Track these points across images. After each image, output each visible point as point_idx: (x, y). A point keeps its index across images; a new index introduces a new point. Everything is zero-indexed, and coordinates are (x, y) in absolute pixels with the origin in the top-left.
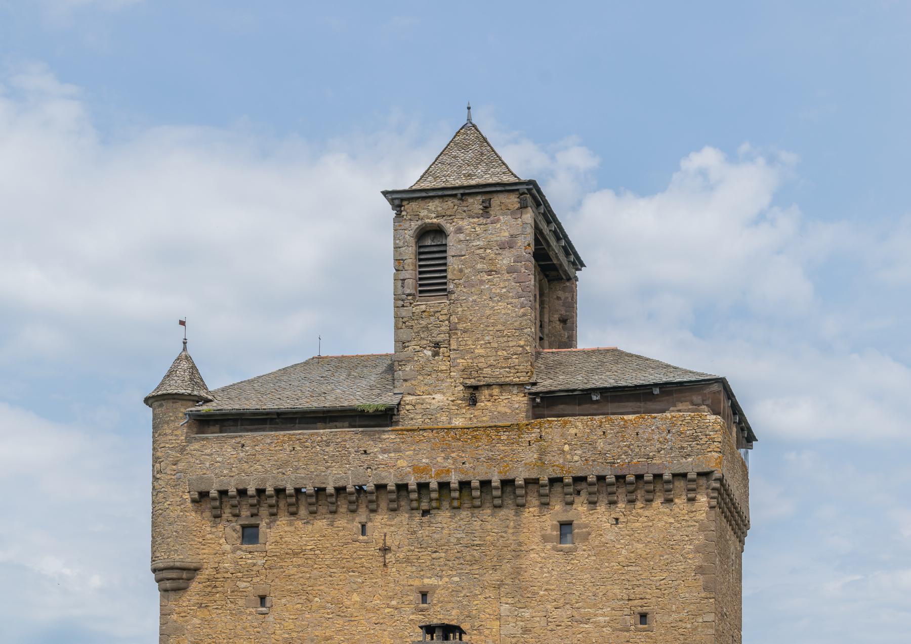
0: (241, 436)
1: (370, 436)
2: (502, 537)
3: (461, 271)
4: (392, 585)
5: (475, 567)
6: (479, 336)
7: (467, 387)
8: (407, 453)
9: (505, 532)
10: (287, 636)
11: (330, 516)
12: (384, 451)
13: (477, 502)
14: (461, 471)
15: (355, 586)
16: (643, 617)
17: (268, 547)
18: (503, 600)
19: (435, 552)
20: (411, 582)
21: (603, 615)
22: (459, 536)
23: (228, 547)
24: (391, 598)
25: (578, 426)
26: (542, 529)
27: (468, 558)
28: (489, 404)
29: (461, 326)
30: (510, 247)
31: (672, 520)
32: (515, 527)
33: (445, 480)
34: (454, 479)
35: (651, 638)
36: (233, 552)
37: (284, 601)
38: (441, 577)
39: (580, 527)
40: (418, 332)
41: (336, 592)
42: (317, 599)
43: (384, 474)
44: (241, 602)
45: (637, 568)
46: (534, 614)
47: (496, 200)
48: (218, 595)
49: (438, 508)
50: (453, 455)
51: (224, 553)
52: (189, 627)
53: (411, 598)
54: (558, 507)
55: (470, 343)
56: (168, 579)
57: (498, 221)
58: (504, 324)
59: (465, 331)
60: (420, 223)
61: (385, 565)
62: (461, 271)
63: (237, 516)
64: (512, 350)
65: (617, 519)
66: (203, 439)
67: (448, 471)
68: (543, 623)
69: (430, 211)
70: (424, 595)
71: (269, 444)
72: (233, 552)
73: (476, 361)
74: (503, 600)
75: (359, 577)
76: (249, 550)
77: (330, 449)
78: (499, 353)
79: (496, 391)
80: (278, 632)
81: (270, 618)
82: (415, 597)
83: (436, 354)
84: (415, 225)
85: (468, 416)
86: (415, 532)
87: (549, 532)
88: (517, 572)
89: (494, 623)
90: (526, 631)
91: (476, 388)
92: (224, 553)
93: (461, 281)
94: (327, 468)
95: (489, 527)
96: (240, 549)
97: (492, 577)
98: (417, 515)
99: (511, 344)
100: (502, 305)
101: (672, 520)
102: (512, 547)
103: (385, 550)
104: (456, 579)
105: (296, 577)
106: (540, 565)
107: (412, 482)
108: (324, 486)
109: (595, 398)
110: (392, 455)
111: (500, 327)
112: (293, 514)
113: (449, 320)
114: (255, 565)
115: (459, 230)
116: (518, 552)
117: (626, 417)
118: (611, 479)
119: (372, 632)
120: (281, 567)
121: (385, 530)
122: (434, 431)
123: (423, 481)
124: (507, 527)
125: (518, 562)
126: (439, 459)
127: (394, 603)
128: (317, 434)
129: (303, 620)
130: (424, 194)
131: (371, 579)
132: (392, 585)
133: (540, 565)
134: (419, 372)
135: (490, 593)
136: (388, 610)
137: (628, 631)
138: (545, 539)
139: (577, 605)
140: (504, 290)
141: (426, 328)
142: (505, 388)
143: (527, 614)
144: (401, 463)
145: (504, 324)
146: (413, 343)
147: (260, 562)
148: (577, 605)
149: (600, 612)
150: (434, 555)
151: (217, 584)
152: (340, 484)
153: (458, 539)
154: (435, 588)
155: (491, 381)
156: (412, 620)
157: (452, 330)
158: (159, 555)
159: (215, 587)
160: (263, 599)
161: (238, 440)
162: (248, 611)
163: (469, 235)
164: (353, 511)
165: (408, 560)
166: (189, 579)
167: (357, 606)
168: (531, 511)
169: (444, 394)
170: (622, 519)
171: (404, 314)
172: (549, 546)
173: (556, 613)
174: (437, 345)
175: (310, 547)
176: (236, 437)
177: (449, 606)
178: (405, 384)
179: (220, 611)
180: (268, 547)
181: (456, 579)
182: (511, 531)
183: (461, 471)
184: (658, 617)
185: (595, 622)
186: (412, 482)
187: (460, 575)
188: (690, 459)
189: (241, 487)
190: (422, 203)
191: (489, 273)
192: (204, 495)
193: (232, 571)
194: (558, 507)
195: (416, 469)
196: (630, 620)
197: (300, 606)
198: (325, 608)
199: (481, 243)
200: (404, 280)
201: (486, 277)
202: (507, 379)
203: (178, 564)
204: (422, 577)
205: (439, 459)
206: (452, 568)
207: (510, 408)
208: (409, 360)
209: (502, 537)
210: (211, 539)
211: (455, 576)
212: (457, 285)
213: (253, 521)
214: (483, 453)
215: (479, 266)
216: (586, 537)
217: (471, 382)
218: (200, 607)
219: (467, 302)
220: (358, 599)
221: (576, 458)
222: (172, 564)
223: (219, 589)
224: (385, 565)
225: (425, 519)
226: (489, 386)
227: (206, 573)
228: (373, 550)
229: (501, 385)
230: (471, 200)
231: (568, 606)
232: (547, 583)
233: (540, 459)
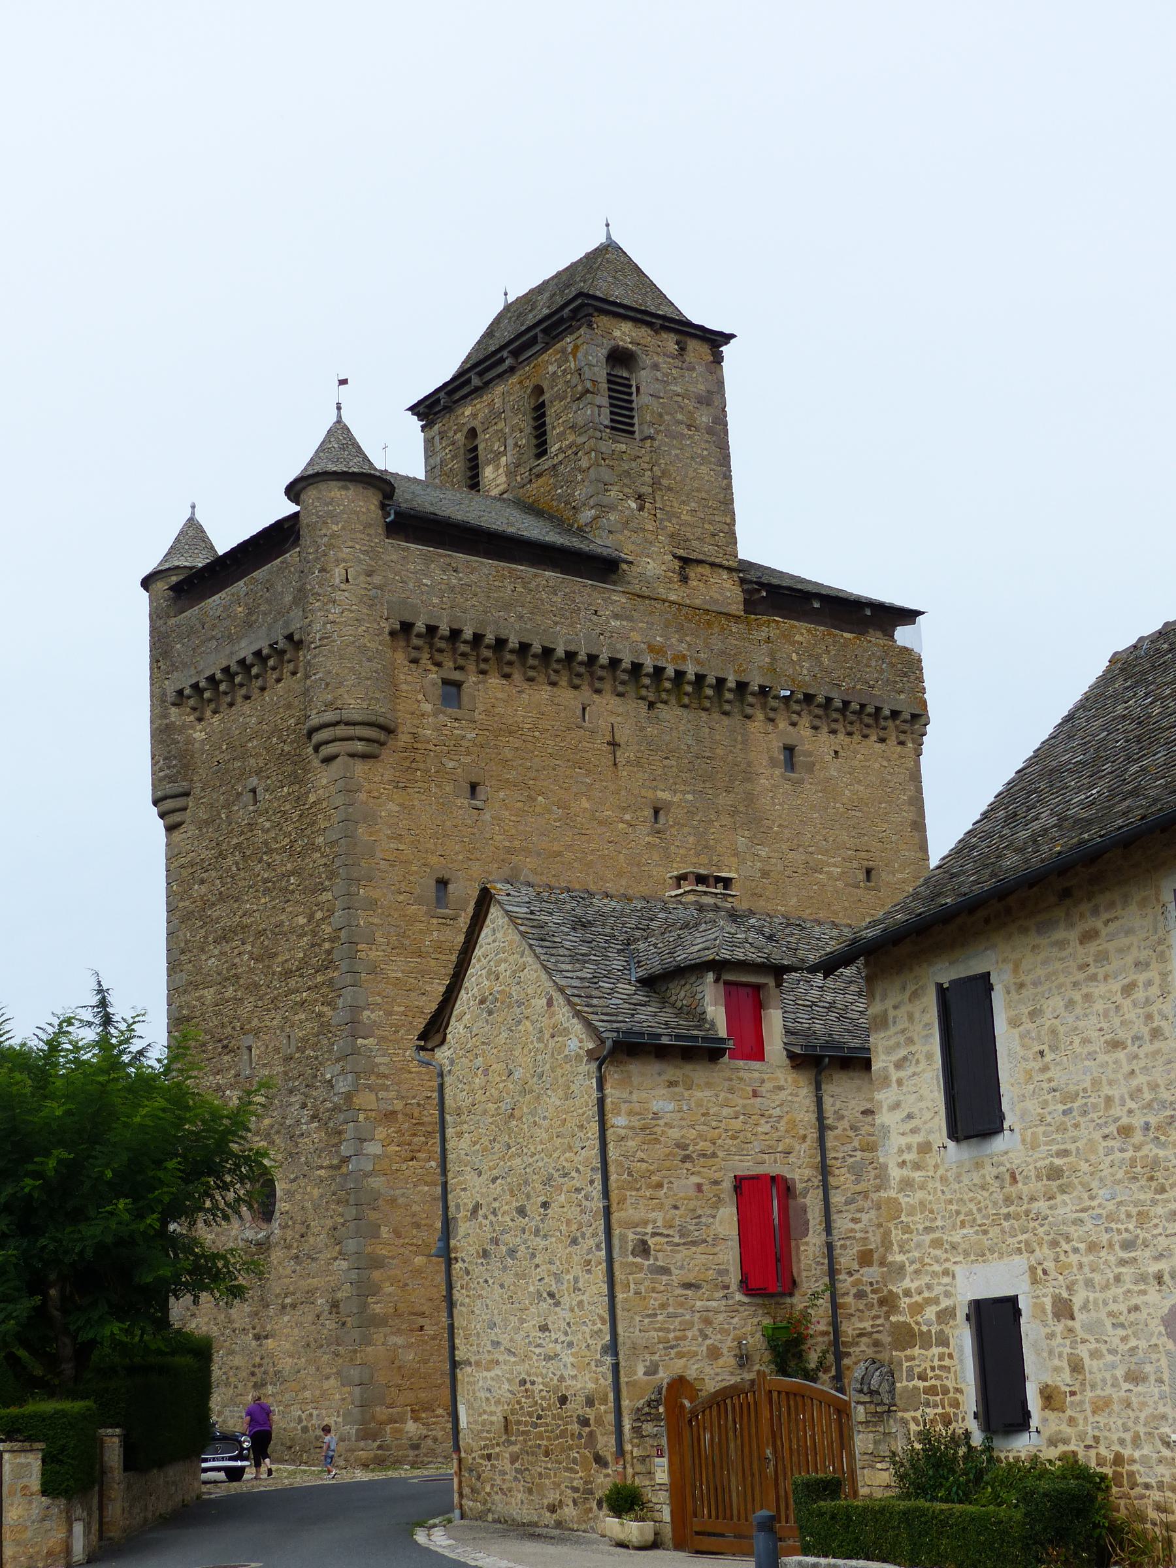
0: (449, 556)
1: (600, 593)
2: (731, 751)
3: (661, 415)
4: (623, 793)
5: (708, 785)
6: (684, 498)
7: (680, 558)
8: (641, 625)
9: (734, 746)
10: (508, 844)
11: (549, 688)
12: (616, 616)
13: (707, 704)
14: (698, 662)
15: (584, 789)
16: (868, 872)
17: (476, 715)
18: (739, 831)
19: (666, 758)
20: (643, 793)
21: (835, 865)
22: (689, 742)
23: (427, 707)
24: (624, 810)
25: (803, 632)
26: (769, 750)
27: (700, 772)
28: (701, 585)
29: (665, 482)
30: (708, 405)
31: (885, 763)
32: (742, 743)
33: (682, 668)
34: (691, 670)
35: (879, 898)
36: (435, 715)
37: (502, 794)
38: (675, 792)
39: (805, 756)
40: (619, 476)
41: (563, 791)
42: (540, 798)
43: (619, 646)
44: (448, 788)
45: (860, 814)
46: (771, 855)
47: (693, 345)
48: (419, 773)
49: (665, 703)
50: (688, 639)
51: (423, 715)
52: (383, 814)
53: (646, 814)
54: (782, 725)
55: (676, 505)
56: (360, 739)
57: (693, 369)
58: (708, 492)
59: (670, 489)
60: (613, 342)
61: (615, 764)
62: (661, 415)
63: (438, 665)
64: (718, 527)
65: (836, 752)
66: (404, 550)
67: (684, 657)
68: (780, 868)
69: (624, 333)
70: (656, 812)
71: (487, 576)
72: (435, 715)
73: (683, 528)
74: (739, 831)
75: (587, 775)
76: (454, 716)
77: (558, 599)
78: (706, 526)
79: (707, 570)
80: (497, 838)
81: (487, 816)
82: (649, 813)
83: (641, 509)
84: (608, 345)
85: (681, 594)
86: (642, 729)
87: (776, 754)
88: (750, 798)
89: (732, 859)
90: (765, 874)
91: (685, 561)
92: (423, 715)
93: (662, 428)
94: (556, 623)
95: (718, 737)
96: (444, 713)
97: (724, 800)
98: (643, 706)
99: (717, 519)
100: (703, 469)
101: (885, 763)
102: (743, 766)
103: (613, 744)
104: (690, 797)
105: (515, 764)
106: (771, 794)
107: (648, 662)
108: (552, 646)
109: (816, 605)
110: (625, 623)
111: (703, 495)
112: (507, 676)
113: (651, 470)
114: (463, 737)
115: (656, 367)
116: (749, 776)
117: (845, 635)
118: (838, 704)
119: (606, 852)
120: (496, 748)
121: (612, 720)
122: (667, 604)
123: (659, 664)
124: (735, 740)
125: (749, 786)
126: (673, 640)
127: (627, 817)
128: (541, 576)
129: (526, 825)
130: (621, 311)
131: (601, 781)
132: (623, 793)
133: (771, 794)
134: (625, 525)
135: (726, 820)
136: (621, 825)
137: (859, 887)
138: (773, 762)
139: (810, 849)
140: (705, 453)
141: (627, 473)
142: (716, 569)
143: (764, 852)
144: (635, 636)
145: (708, 492)
146: (616, 488)
147: (470, 736)
148: (810, 849)
149: (832, 860)
150: (666, 762)
151: (418, 757)
152: (572, 648)
153: (689, 746)
154: (668, 805)
155: (701, 557)
156: (648, 843)
157: (655, 483)
158: (353, 701)
159: (414, 760)
160: (474, 787)
161: (448, 560)
162: (459, 802)
163: (667, 375)
164: (576, 687)
165: (638, 763)
166: (382, 744)
167: (587, 815)
168: (757, 724)
169: (654, 560)
170: (841, 754)
171: (603, 449)
172: (778, 772)
173: (792, 855)
174: (640, 497)
175: (528, 726)
176: (445, 556)
177: (686, 830)
178: (611, 536)
179: (424, 797)
180: (476, 715)
181: (690, 797)
182: (740, 746)
183: (698, 662)
184: (884, 875)
185: (828, 873)
186: (648, 662)
187: (694, 792)
188: (902, 696)
189: (455, 626)
190: (614, 321)
191: (689, 427)
192: (407, 627)
193: (435, 742)
194: (782, 725)
195: (651, 648)
196: (861, 876)
197: (520, 805)
198: (549, 811)
199: (678, 389)
200: (599, 407)
201: (686, 431)
202: (717, 560)
203: (381, 720)
204: (655, 789)
205: (673, 640)
206: (685, 783)
207: (722, 594)
208: (612, 508)
209: (731, 751)
210: (407, 691)
211: (689, 793)
212: (658, 432)
213: (457, 676)
214: (718, 646)
215: (679, 417)
216: (810, 768)
217: (681, 552)
218: (397, 787)
219: (670, 454)
220: (587, 805)
221: (805, 672)
222: (374, 718)
223: (422, 766)
224: (615, 764)
225: (653, 713)
226: (700, 562)
227: (404, 738)
228: (600, 744)
229: (713, 565)
230: (664, 335)
231: (801, 849)
232: (780, 816)
233: (771, 664)
